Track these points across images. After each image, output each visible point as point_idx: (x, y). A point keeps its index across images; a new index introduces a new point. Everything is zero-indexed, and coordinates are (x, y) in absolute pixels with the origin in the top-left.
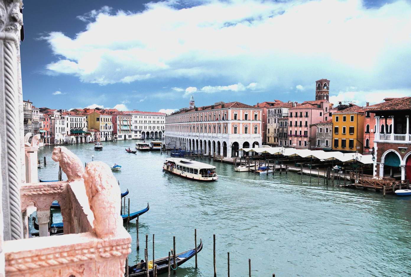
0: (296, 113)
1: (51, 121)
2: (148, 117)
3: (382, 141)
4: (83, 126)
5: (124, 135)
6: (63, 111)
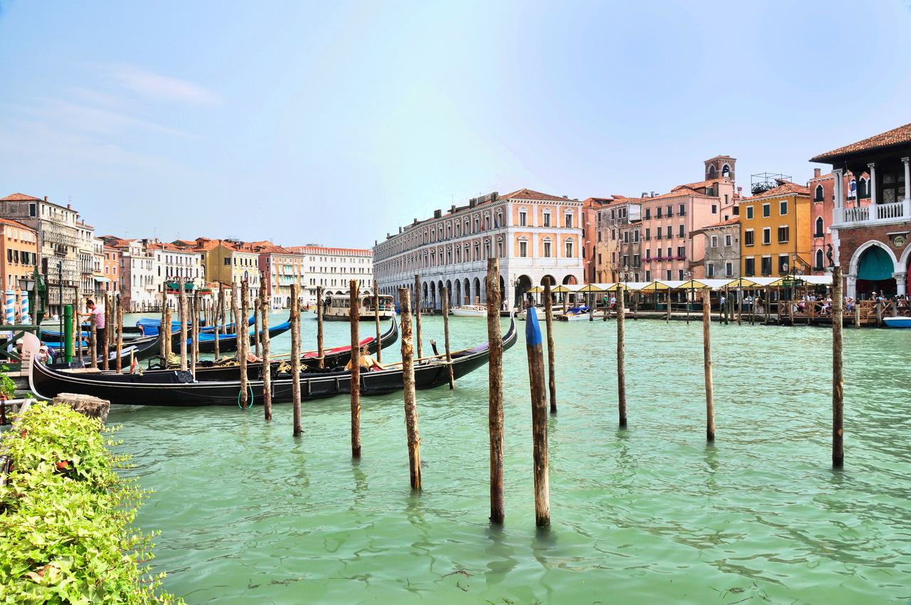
0: (659, 210)
1: (123, 261)
2: (338, 259)
3: (850, 224)
4: (194, 275)
6: (151, 241)
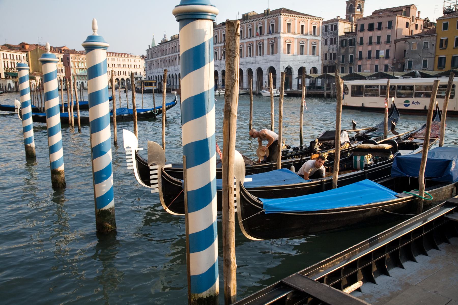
5: (81, 82)
